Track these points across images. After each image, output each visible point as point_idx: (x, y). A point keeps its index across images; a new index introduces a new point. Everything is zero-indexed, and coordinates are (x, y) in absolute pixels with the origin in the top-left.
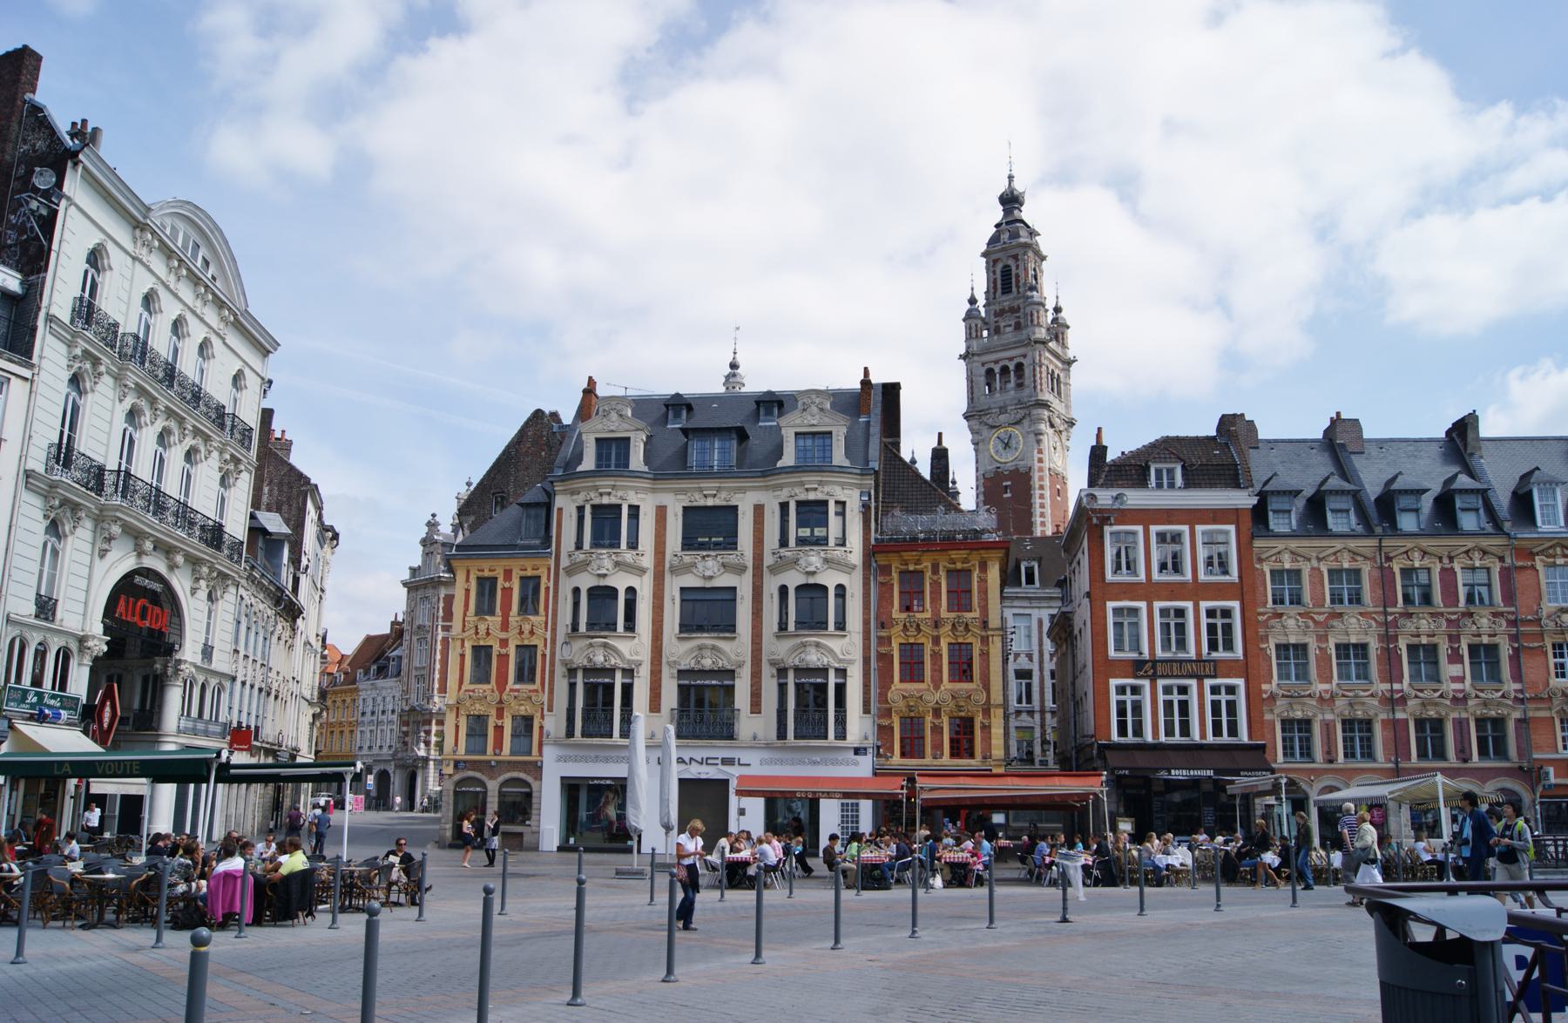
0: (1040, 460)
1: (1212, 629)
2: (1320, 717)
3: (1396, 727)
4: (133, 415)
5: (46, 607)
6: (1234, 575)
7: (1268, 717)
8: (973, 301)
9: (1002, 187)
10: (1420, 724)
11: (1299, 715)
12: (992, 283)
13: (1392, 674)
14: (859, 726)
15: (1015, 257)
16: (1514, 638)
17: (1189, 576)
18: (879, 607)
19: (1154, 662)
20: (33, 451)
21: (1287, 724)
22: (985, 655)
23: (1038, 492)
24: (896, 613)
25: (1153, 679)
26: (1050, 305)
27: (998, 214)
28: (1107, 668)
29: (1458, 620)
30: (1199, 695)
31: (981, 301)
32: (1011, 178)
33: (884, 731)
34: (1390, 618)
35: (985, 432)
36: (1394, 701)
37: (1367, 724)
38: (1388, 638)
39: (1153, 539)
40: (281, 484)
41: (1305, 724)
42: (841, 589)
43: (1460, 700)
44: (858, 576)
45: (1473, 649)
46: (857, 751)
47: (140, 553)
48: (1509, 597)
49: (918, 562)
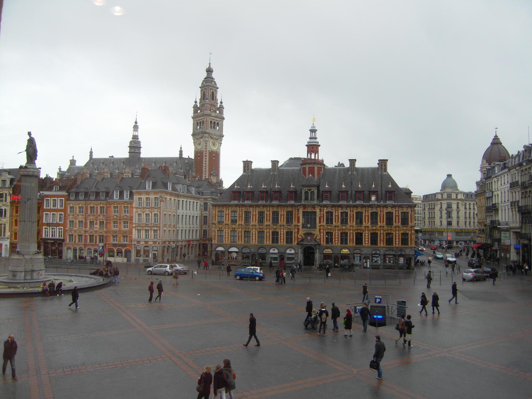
0: (206, 148)
1: (60, 217)
3: (85, 236)
8: (196, 102)
9: (208, 67)
10: (91, 236)
12: (201, 96)
13: (86, 227)
14: (8, 234)
15: (206, 89)
16: (106, 220)
19: (50, 223)
21: (70, 235)
23: (204, 158)
24: (14, 214)
25: (50, 226)
26: (219, 102)
27: (205, 75)
28: (44, 225)
30: (57, 229)
31: (198, 101)
32: (210, 64)
33: (11, 235)
35: (196, 140)
36: (86, 232)
37: (82, 235)
38: (86, 220)
41: (72, 235)
42: (5, 210)
43: (96, 232)
44: (9, 207)
45: (100, 222)
46: (8, 238)
48: (106, 213)
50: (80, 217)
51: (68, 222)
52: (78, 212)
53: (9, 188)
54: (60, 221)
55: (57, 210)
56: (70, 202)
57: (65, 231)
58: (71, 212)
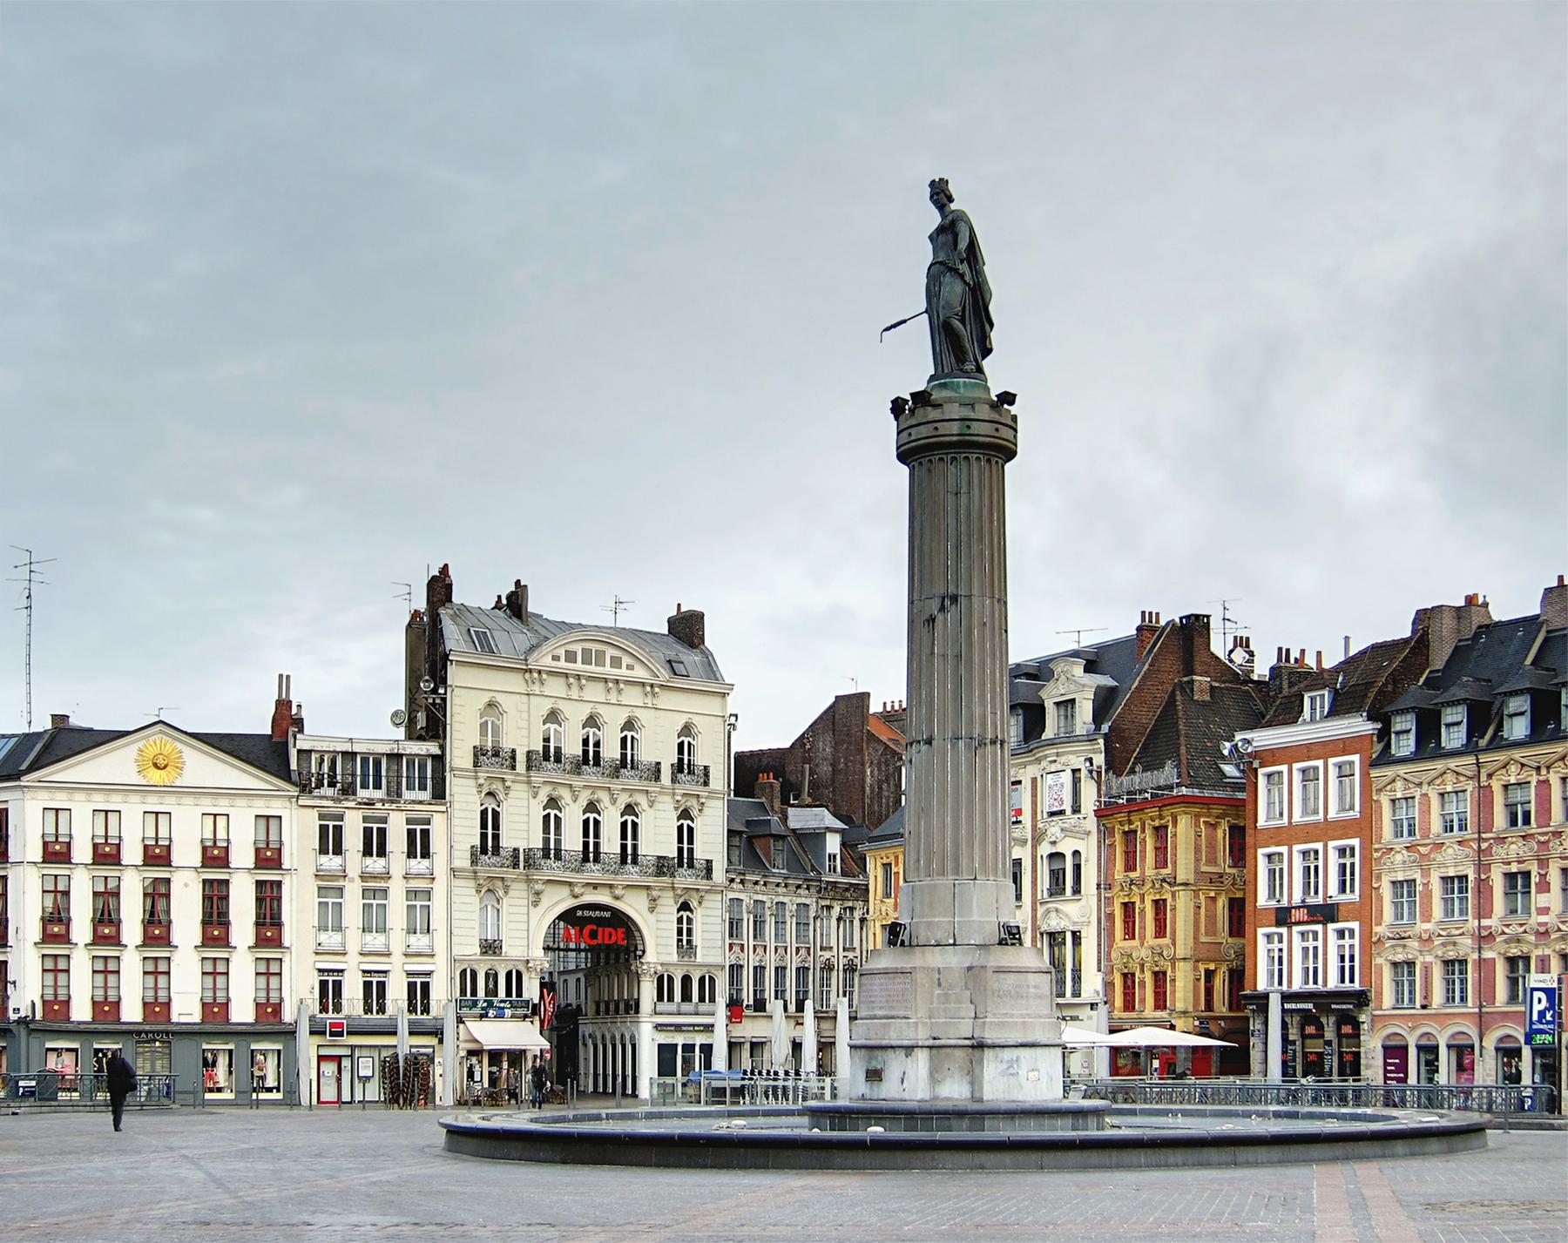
2: (1421, 959)
4: (553, 802)
5: (491, 947)
6: (1356, 813)
7: (1378, 961)
11: (1399, 958)
13: (1483, 911)
17: (1321, 816)
18: (1107, 869)
20: (456, 854)
22: (1174, 909)
25: (1290, 925)
29: (1547, 842)
34: (1484, 846)
36: (1484, 938)
37: (1463, 962)
38: (1482, 867)
39: (1297, 777)
40: (879, 763)
42: (1076, 853)
44: (1093, 839)
47: (575, 897)
49: (1130, 822)
50: (1451, 851)
51: (1386, 892)
52: (1436, 825)
53: (1090, 739)
54: (1343, 890)
55: (1326, 830)
56: (1390, 771)
57: (1370, 944)
58: (1398, 833)
